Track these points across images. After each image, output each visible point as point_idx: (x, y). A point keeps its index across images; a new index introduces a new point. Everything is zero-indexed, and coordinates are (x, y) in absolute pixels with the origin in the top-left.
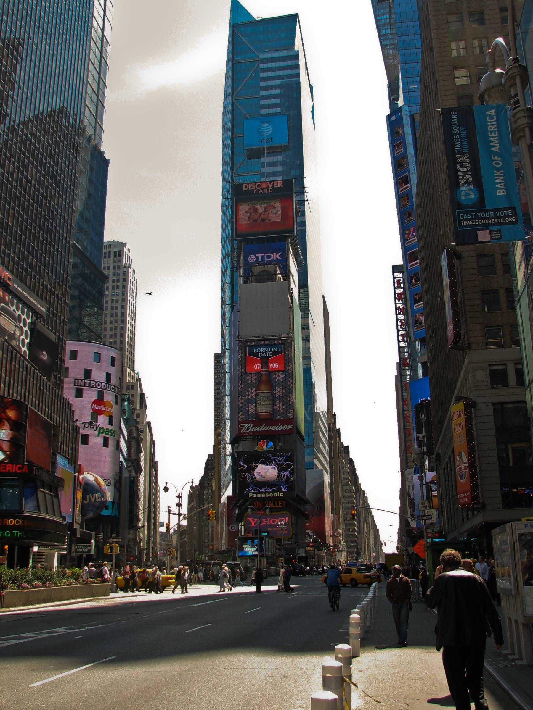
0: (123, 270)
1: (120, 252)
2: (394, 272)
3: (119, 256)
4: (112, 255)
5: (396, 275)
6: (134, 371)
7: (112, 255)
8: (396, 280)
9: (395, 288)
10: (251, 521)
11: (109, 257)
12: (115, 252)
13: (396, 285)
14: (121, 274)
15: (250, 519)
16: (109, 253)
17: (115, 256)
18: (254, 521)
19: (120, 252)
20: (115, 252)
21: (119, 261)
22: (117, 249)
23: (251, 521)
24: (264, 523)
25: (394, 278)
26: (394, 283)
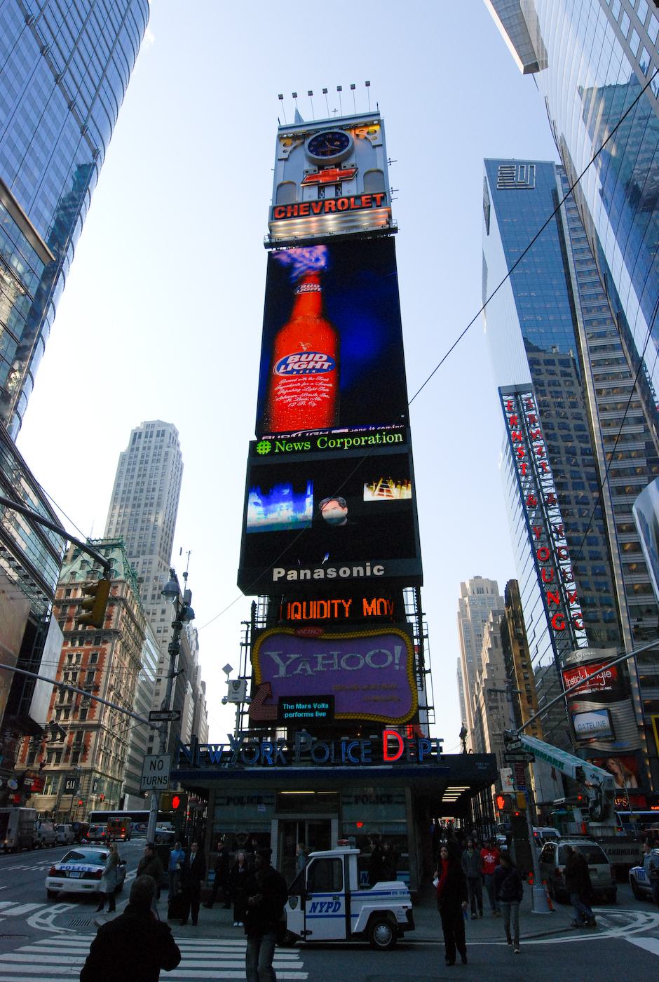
0: (165, 449)
1: (164, 431)
2: (501, 395)
3: (163, 435)
4: (155, 434)
5: (504, 397)
6: (168, 563)
7: (155, 434)
8: (505, 403)
9: (504, 412)
10: (278, 660)
11: (151, 436)
12: (159, 431)
13: (506, 409)
14: (163, 454)
15: (275, 656)
16: (152, 432)
17: (158, 436)
18: (284, 659)
19: (164, 431)
20: (159, 431)
21: (162, 441)
22: (161, 429)
23: (278, 660)
24: (319, 668)
25: (502, 401)
26: (503, 407)
